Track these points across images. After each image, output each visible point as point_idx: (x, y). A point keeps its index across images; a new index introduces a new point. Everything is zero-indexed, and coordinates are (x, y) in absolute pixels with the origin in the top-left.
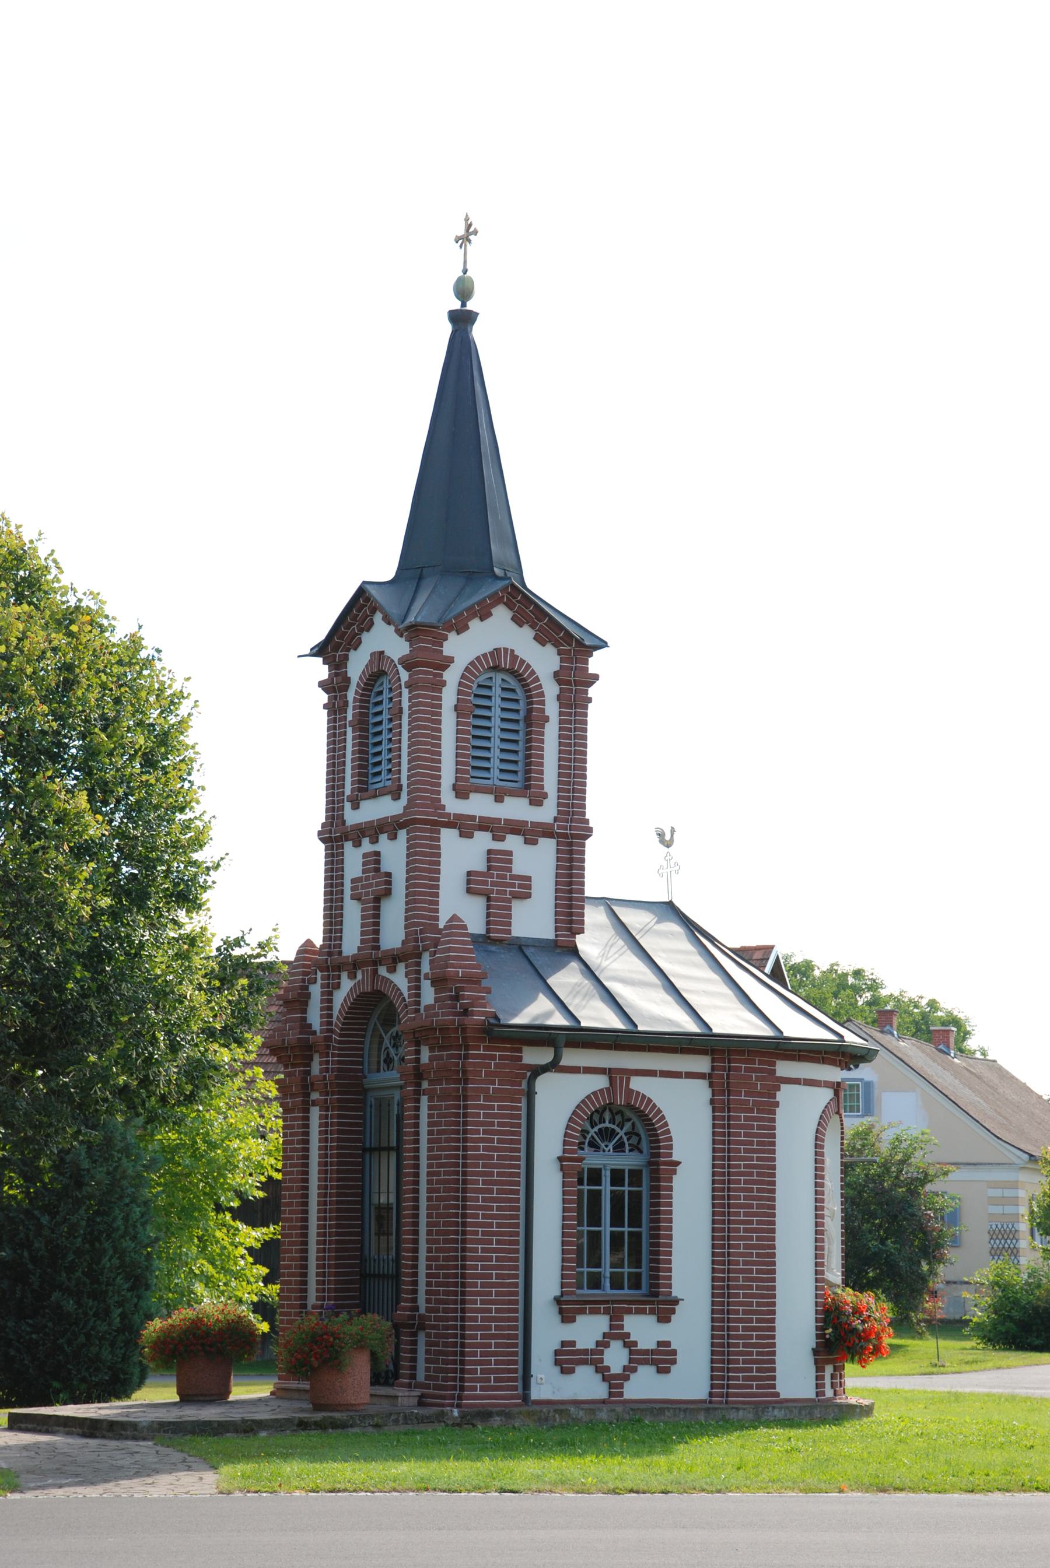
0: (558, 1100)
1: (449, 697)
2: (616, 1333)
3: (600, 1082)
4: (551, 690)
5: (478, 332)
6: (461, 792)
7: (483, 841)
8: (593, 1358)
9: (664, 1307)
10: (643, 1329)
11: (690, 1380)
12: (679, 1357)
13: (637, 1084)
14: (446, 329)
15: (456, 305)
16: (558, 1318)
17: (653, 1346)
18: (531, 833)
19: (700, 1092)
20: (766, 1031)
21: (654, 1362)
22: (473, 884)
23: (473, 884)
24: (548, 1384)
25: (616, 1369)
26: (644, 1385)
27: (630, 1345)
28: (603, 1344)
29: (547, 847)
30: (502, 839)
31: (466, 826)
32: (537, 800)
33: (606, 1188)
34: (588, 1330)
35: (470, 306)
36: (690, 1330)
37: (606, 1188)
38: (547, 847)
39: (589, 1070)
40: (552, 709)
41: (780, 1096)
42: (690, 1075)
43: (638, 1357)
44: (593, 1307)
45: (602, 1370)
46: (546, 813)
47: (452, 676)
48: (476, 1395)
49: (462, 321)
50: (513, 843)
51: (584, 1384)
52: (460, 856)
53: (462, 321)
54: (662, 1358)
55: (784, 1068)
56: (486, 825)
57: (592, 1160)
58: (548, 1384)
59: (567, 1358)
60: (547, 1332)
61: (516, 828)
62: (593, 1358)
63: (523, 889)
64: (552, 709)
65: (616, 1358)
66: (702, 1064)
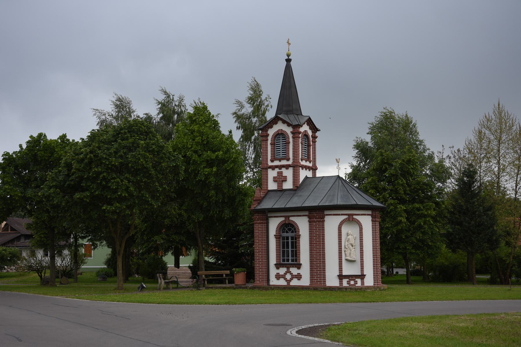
0: (274, 224)
1: (269, 142)
2: (288, 272)
3: (283, 219)
4: (291, 136)
5: (292, 63)
6: (272, 161)
7: (277, 170)
8: (283, 276)
9: (299, 266)
10: (294, 271)
11: (305, 281)
12: (302, 277)
13: (291, 218)
14: (285, 63)
15: (287, 58)
16: (275, 268)
17: (296, 274)
18: (287, 167)
19: (369, 218)
20: (355, 203)
21: (297, 278)
22: (275, 180)
23: (275, 180)
24: (274, 281)
25: (288, 279)
26: (295, 282)
27: (291, 274)
28: (285, 274)
29: (291, 170)
30: (281, 169)
31: (273, 168)
32: (288, 160)
33: (290, 241)
34: (282, 271)
35: (290, 58)
36: (305, 271)
37: (290, 241)
38: (291, 170)
39: (342, 215)
40: (291, 140)
41: (325, 219)
42: (368, 215)
43: (293, 277)
44: (282, 266)
45: (286, 279)
46: (290, 162)
47: (270, 138)
48: (257, 283)
49: (288, 61)
50: (283, 170)
51: (282, 282)
52: (272, 174)
53: (288, 61)
54: (299, 277)
55: (326, 212)
56: (277, 167)
57: (285, 235)
58: (274, 281)
59: (278, 277)
60: (273, 271)
61: (283, 166)
62: (283, 276)
63: (285, 179)
64: (291, 140)
65: (288, 277)
66: (307, 213)
